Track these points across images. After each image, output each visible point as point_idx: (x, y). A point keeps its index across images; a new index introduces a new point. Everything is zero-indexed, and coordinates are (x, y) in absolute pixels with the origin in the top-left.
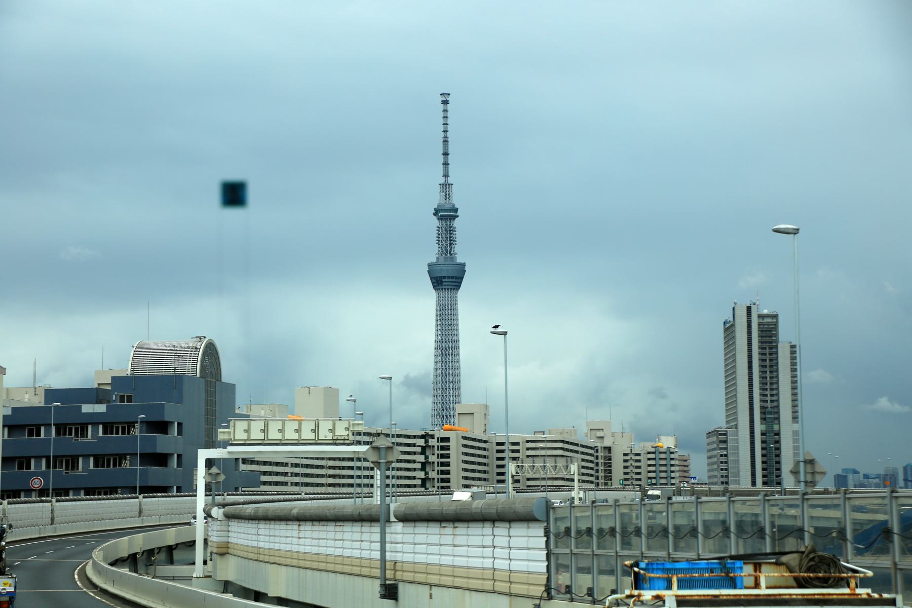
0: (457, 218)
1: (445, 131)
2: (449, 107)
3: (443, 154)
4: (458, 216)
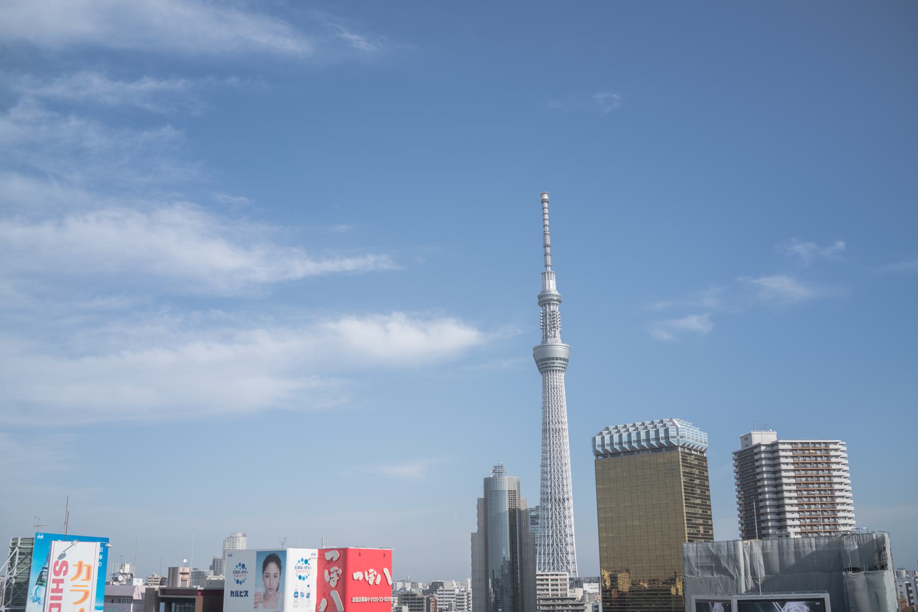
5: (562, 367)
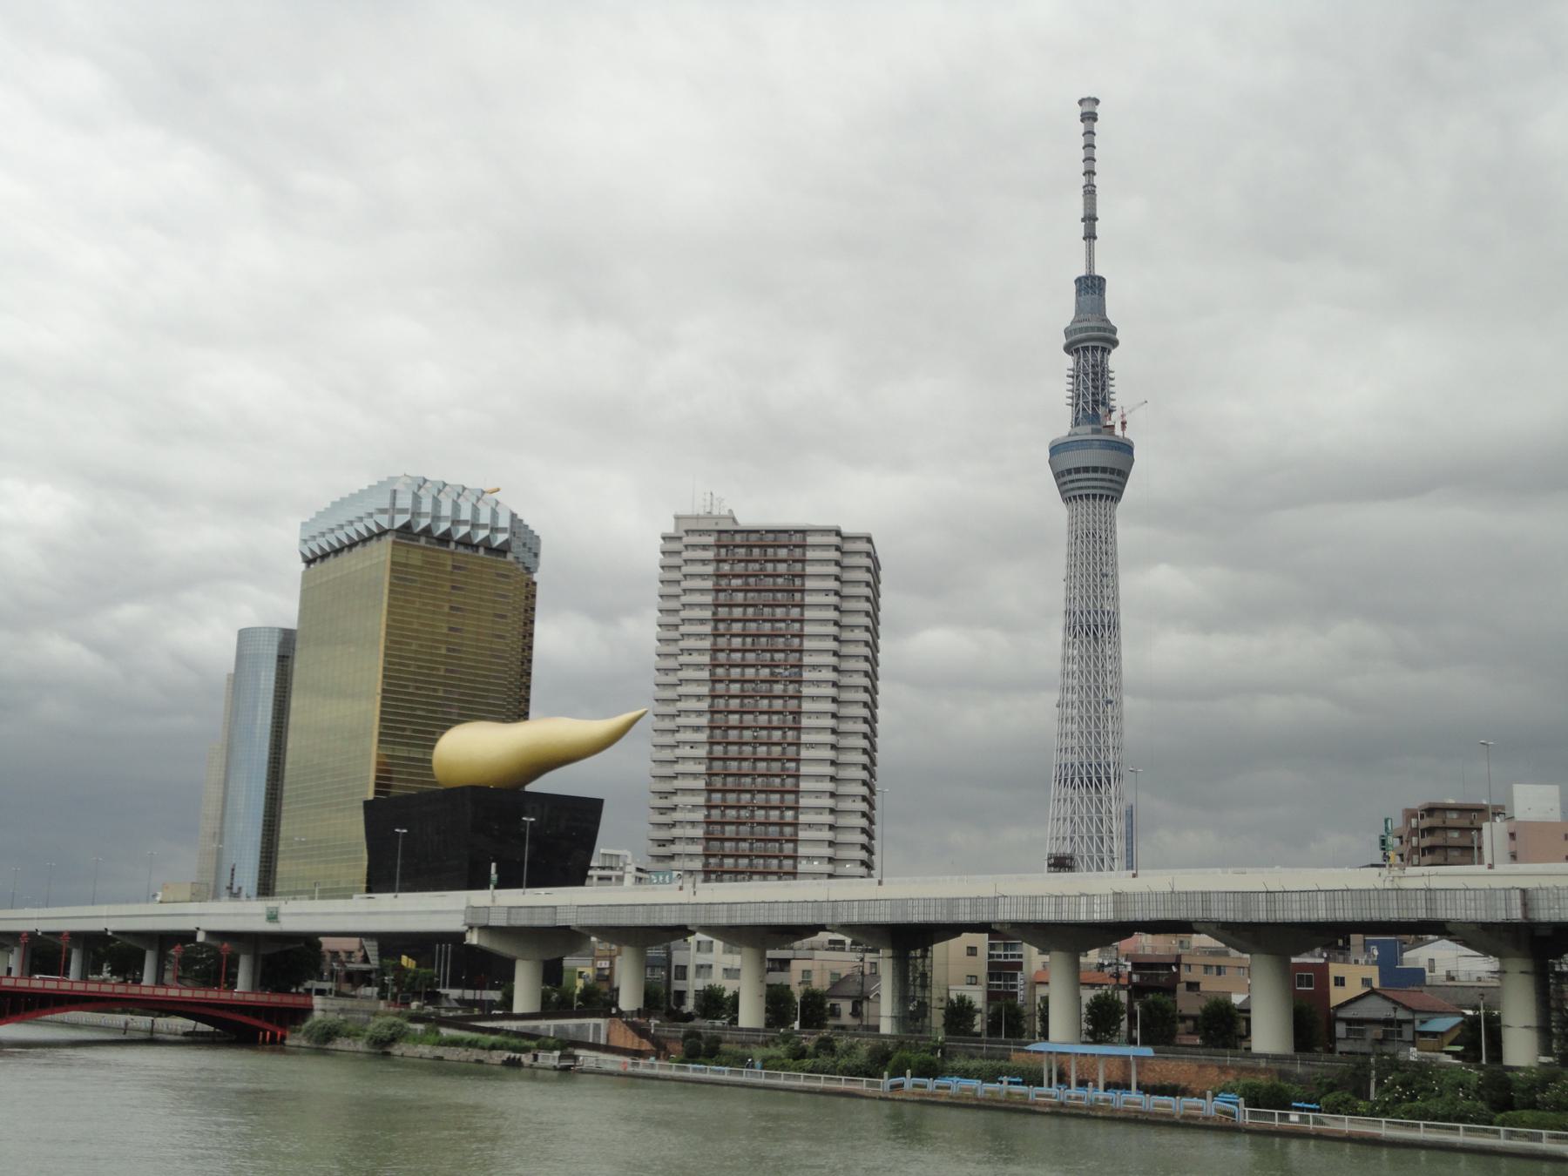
0: (1114, 352)
1: (1090, 173)
2: (1097, 127)
3: (1083, 220)
4: (1115, 343)
5: (1109, 488)
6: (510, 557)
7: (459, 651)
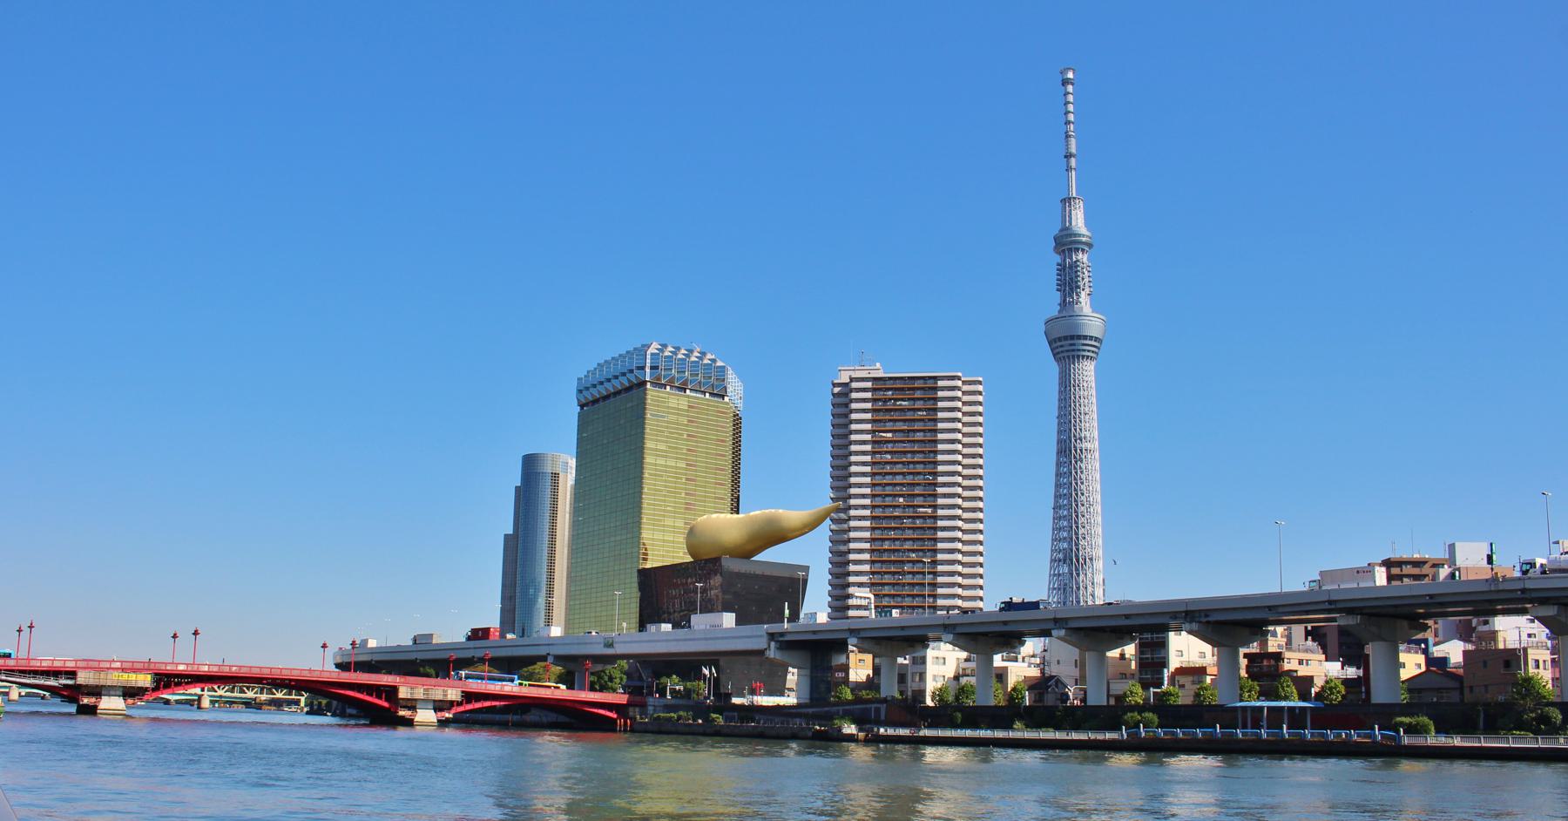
6: (726, 399)
7: (695, 466)
